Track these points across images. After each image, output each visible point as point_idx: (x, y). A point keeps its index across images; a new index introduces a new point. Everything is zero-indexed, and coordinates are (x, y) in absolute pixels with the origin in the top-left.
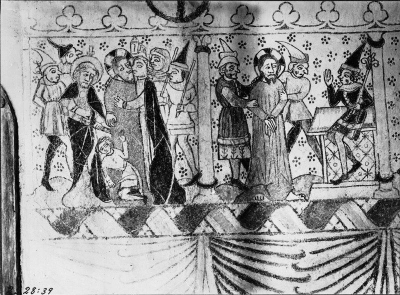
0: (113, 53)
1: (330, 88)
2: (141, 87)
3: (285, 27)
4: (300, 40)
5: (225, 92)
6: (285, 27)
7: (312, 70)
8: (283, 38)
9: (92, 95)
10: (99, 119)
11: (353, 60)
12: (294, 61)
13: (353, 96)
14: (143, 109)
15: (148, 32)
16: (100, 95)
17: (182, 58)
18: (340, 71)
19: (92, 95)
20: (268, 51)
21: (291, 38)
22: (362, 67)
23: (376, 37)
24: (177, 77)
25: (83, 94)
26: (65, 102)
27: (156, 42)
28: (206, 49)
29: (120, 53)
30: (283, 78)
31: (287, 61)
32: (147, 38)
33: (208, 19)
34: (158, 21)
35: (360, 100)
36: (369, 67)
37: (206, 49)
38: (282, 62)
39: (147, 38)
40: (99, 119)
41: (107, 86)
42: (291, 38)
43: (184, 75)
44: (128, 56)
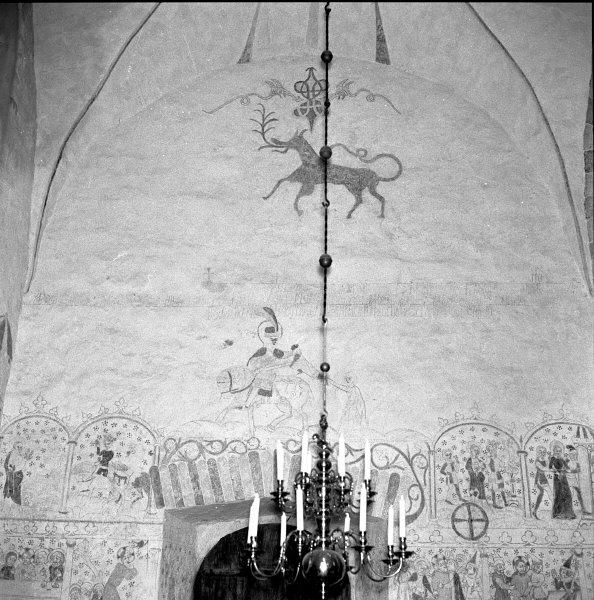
0: (436, 556)
1: (556, 580)
2: (452, 576)
3: (529, 544)
4: (537, 552)
5: (498, 580)
6: (529, 544)
7: (545, 570)
8: (528, 550)
9: (425, 578)
10: (429, 594)
11: (567, 565)
12: (535, 563)
13: (569, 584)
14: (453, 589)
15: (455, 545)
16: (430, 580)
17: (473, 560)
18: (561, 570)
19: (425, 578)
20: (520, 557)
21: (532, 551)
22: (573, 569)
23: (579, 551)
24: (471, 571)
25: (420, 579)
26: (411, 583)
27: (459, 551)
28: (486, 556)
29: (440, 557)
30: (529, 573)
31: (531, 564)
32: (454, 549)
33: (487, 539)
34: (459, 539)
35: (573, 587)
36: (576, 569)
37: (486, 556)
38: (528, 564)
39: (454, 549)
40: (429, 594)
41: (433, 575)
42: (532, 551)
43: (475, 569)
44: (444, 558)
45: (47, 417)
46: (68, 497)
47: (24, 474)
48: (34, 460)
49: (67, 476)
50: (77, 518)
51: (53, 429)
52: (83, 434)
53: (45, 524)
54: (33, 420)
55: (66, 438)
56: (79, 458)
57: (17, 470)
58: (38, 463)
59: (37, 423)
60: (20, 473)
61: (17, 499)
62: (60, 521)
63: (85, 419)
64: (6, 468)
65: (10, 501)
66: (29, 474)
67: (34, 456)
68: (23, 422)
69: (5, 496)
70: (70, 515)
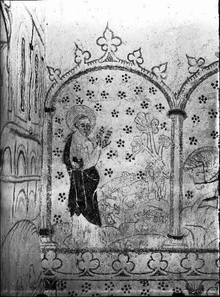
45: (122, 68)
46: (181, 209)
47: (101, 172)
48: (113, 146)
49: (176, 175)
50: (200, 244)
51: (138, 90)
52: (194, 97)
53: (147, 256)
54: (102, 74)
55: (165, 103)
56: (193, 140)
57: (88, 165)
58: (122, 152)
59: (109, 80)
60: (93, 171)
61: (94, 216)
62: (171, 251)
63: (193, 69)
64: (69, 166)
65: (81, 220)
66: (110, 172)
67: (114, 138)
68: (83, 79)
69: (72, 215)
70: (189, 240)
